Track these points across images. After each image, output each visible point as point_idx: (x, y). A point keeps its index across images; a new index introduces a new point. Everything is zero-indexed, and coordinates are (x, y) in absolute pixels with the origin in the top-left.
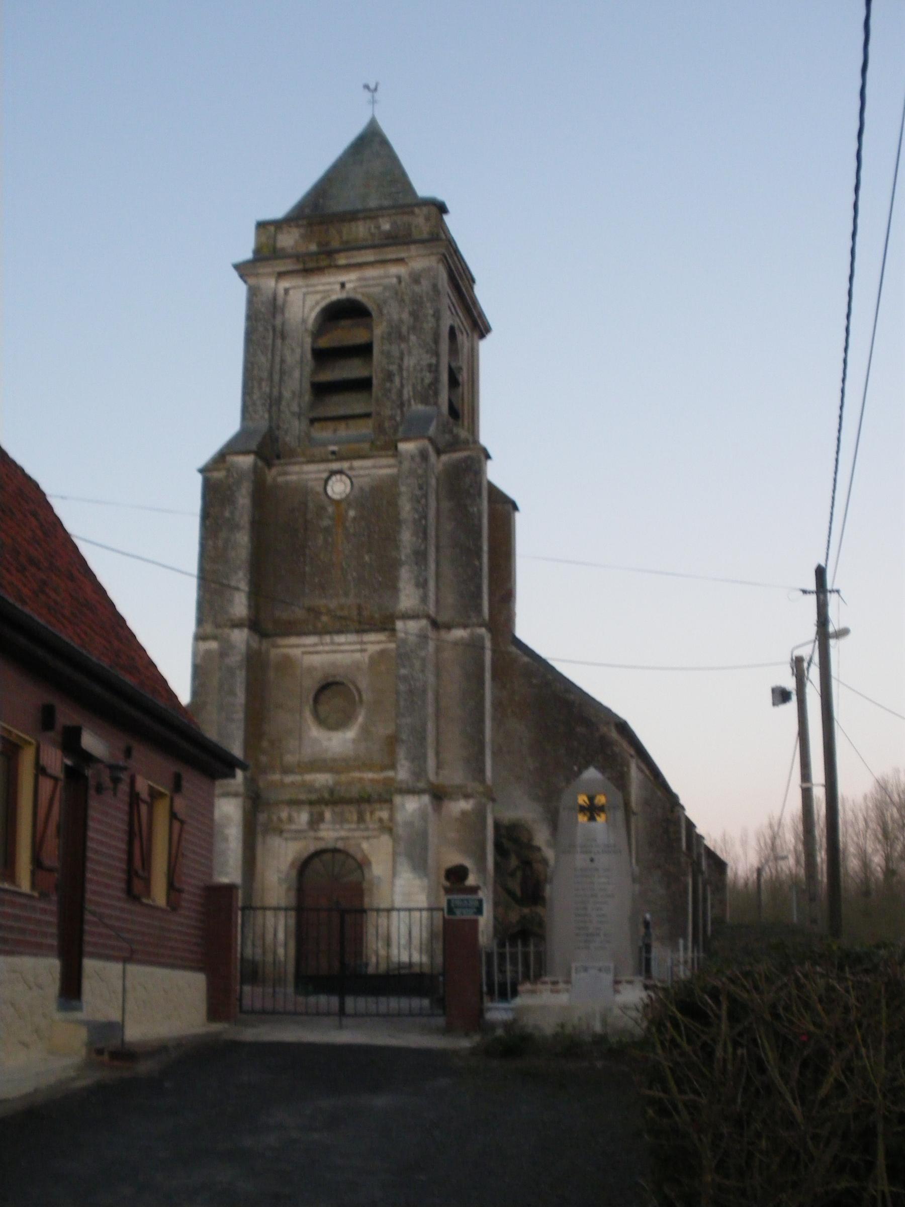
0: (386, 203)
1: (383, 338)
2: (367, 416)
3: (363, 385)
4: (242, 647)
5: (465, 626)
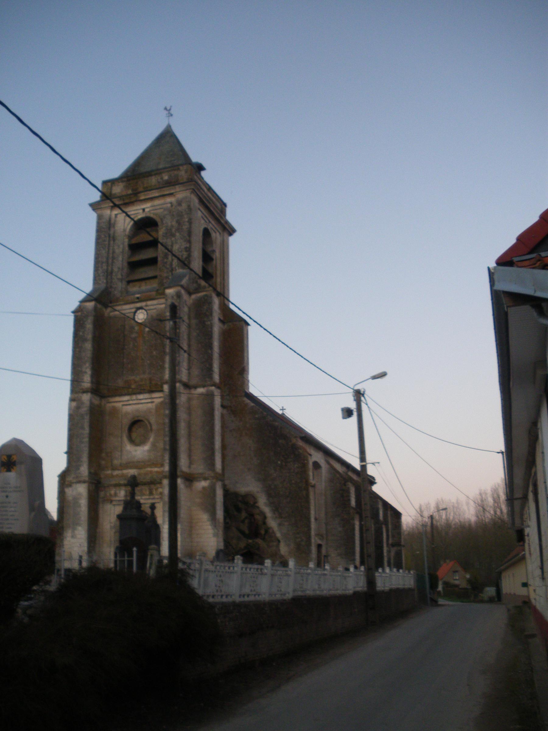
0: (168, 166)
1: (163, 236)
2: (155, 277)
3: (153, 261)
4: (87, 403)
5: (204, 386)
